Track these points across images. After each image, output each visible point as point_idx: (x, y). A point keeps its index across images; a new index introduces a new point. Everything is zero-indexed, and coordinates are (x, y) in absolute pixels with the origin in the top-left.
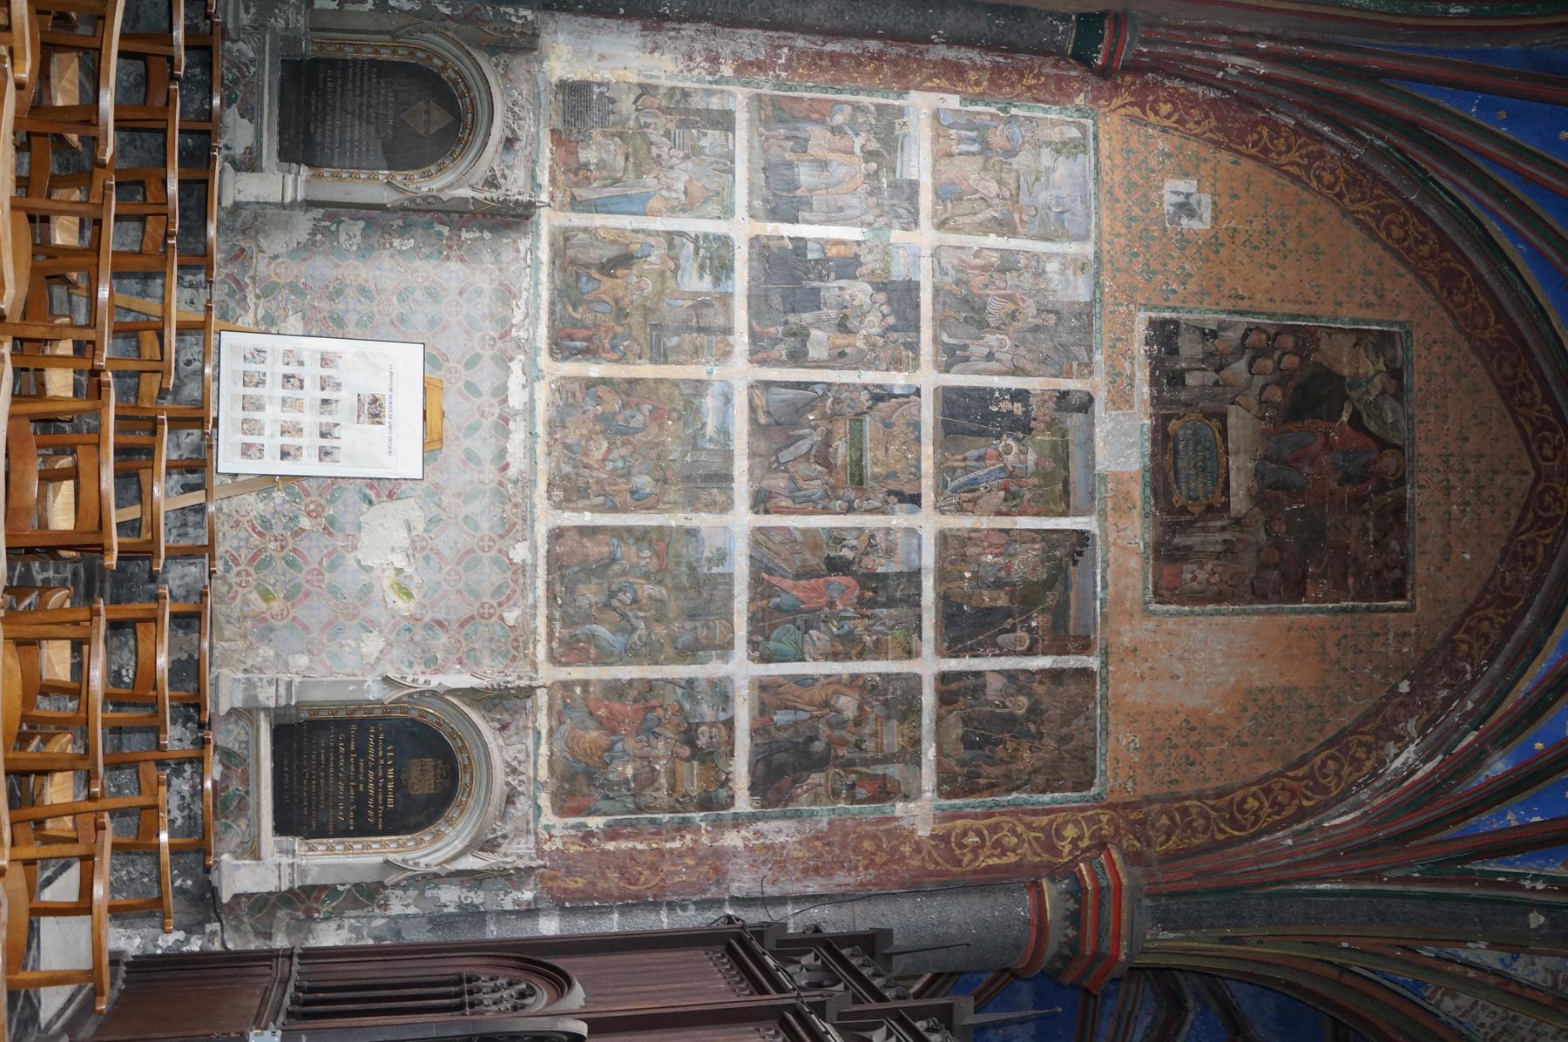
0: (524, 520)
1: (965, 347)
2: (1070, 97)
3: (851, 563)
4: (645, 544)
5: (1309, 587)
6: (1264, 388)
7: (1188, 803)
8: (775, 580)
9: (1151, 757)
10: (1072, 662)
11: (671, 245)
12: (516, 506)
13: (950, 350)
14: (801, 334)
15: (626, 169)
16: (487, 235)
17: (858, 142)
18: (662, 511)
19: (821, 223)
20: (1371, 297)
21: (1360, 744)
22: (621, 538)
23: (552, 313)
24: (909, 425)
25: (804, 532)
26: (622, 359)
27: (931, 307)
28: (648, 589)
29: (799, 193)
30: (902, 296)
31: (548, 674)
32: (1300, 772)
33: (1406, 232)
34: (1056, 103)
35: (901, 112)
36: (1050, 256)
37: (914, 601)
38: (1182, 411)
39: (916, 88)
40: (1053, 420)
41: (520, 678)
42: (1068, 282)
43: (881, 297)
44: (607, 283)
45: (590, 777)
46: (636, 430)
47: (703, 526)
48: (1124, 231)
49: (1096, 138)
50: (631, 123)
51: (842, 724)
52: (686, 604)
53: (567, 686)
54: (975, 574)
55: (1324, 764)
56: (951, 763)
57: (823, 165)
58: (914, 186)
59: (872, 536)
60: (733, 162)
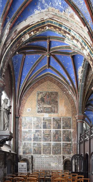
14: (39, 138)
30: (36, 131)
31: (62, 155)
53: (63, 154)
58: (29, 130)
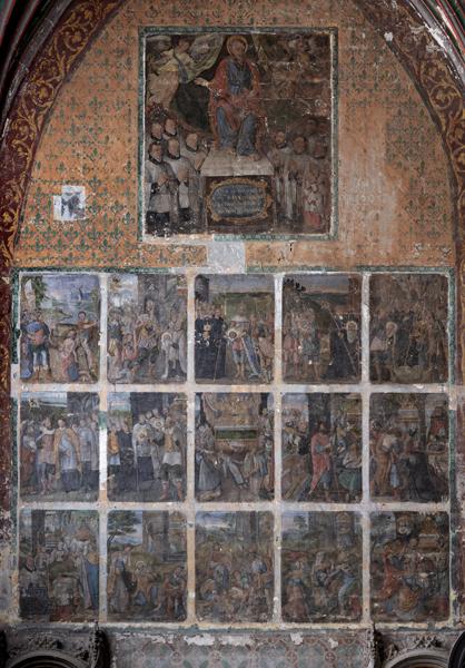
0: (279, 635)
1: (170, 363)
2: (6, 287)
3: (303, 438)
4: (292, 565)
5: (320, 114)
6: (188, 148)
7: (459, 207)
8: (313, 486)
9: (428, 234)
10: (365, 290)
11: (116, 549)
12: (270, 641)
13: (173, 373)
14: (166, 469)
15: (71, 577)
16: (114, 659)
17: (46, 431)
18: (273, 555)
19: (98, 456)
20: (123, 60)
21: (426, 73)
22: (288, 579)
23: (159, 620)
24: (219, 401)
25: (284, 467)
26: (185, 578)
27: (147, 386)
28: (318, 563)
29: (80, 470)
30: (140, 404)
31: (366, 623)
32: (443, 121)
33: (77, 30)
34: (10, 298)
35: (24, 403)
36: (110, 304)
37: (326, 397)
38: (205, 210)
39: (9, 393)
40: (213, 303)
41: (369, 639)
42: (126, 291)
43: (142, 418)
44: (140, 587)
45: (427, 598)
46: (226, 570)
47: (281, 530)
48: (90, 250)
49: (31, 269)
50: (43, 573)
51: (399, 444)
52: (327, 541)
53: (373, 612)
54: (311, 357)
55: (438, 102)
56: (426, 374)
57: (62, 454)
58: (71, 395)
59: (287, 424)
60: (63, 511)
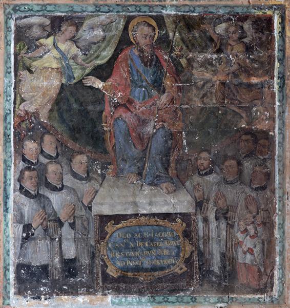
5: (259, 127)
6: (75, 175)
38: (98, 262)
